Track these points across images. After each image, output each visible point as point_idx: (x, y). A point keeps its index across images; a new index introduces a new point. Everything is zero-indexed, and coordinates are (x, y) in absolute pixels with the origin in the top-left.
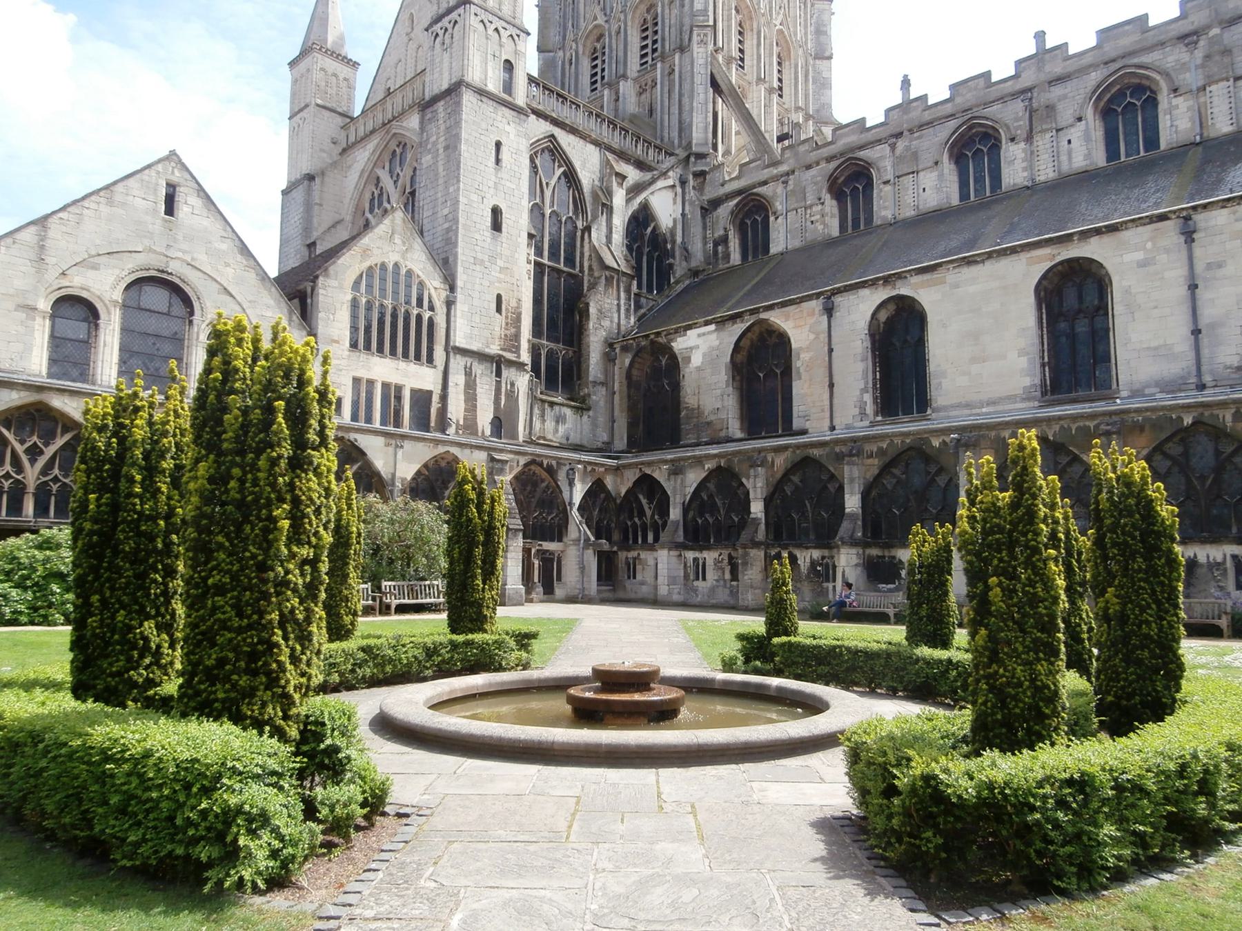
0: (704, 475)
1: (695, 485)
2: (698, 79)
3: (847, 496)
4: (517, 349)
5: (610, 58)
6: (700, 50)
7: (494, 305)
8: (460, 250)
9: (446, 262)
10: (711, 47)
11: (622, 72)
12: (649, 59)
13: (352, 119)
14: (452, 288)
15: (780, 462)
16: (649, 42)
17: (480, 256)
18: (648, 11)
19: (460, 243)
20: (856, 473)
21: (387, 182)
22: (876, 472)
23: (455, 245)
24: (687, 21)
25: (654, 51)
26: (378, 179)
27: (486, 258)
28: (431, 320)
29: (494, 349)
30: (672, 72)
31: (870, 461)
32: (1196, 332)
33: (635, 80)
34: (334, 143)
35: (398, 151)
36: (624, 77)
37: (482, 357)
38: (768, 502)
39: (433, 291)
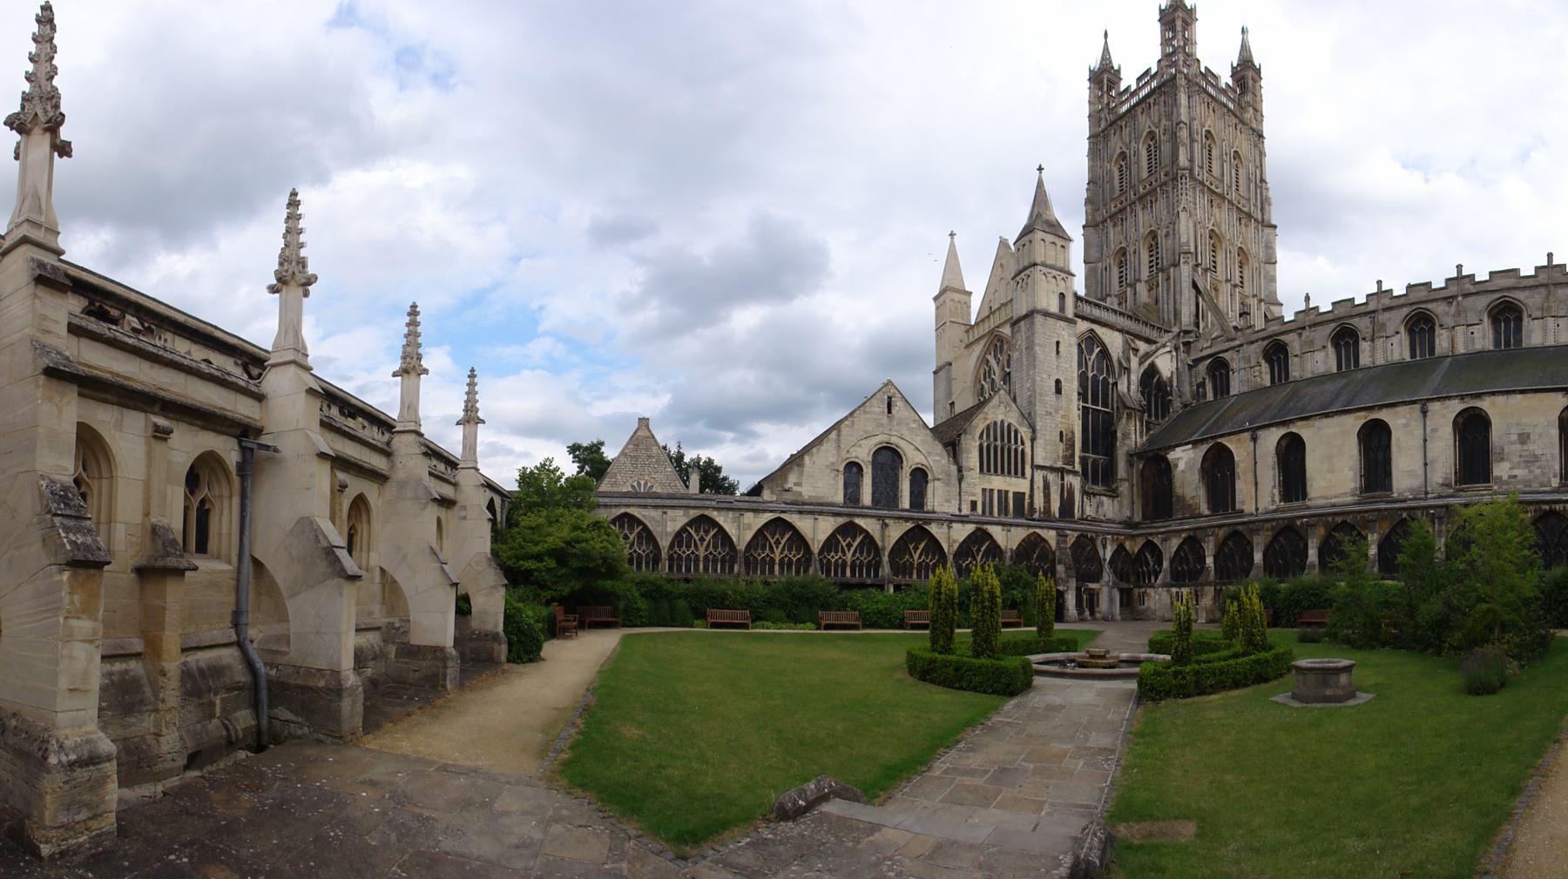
0: (1181, 540)
1: (1176, 547)
2: (1184, 285)
3: (1255, 553)
4: (1073, 464)
5: (1131, 268)
6: (1186, 267)
7: (1058, 438)
8: (1037, 408)
9: (1030, 414)
10: (1192, 263)
11: (1137, 277)
12: (1154, 268)
13: (970, 325)
14: (1034, 431)
15: (1222, 533)
16: (1154, 258)
17: (1049, 410)
18: (1153, 240)
19: (1038, 404)
20: (1260, 541)
21: (993, 362)
22: (1271, 539)
23: (1035, 405)
24: (1177, 247)
25: (1157, 264)
26: (988, 361)
27: (1053, 411)
28: (1023, 451)
29: (1059, 464)
30: (1168, 279)
31: (1267, 533)
32: (1426, 464)
33: (1146, 282)
34: (961, 341)
35: (998, 344)
36: (1139, 280)
37: (1052, 469)
38: (1216, 557)
39: (1023, 434)
